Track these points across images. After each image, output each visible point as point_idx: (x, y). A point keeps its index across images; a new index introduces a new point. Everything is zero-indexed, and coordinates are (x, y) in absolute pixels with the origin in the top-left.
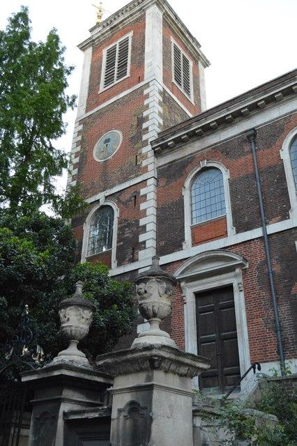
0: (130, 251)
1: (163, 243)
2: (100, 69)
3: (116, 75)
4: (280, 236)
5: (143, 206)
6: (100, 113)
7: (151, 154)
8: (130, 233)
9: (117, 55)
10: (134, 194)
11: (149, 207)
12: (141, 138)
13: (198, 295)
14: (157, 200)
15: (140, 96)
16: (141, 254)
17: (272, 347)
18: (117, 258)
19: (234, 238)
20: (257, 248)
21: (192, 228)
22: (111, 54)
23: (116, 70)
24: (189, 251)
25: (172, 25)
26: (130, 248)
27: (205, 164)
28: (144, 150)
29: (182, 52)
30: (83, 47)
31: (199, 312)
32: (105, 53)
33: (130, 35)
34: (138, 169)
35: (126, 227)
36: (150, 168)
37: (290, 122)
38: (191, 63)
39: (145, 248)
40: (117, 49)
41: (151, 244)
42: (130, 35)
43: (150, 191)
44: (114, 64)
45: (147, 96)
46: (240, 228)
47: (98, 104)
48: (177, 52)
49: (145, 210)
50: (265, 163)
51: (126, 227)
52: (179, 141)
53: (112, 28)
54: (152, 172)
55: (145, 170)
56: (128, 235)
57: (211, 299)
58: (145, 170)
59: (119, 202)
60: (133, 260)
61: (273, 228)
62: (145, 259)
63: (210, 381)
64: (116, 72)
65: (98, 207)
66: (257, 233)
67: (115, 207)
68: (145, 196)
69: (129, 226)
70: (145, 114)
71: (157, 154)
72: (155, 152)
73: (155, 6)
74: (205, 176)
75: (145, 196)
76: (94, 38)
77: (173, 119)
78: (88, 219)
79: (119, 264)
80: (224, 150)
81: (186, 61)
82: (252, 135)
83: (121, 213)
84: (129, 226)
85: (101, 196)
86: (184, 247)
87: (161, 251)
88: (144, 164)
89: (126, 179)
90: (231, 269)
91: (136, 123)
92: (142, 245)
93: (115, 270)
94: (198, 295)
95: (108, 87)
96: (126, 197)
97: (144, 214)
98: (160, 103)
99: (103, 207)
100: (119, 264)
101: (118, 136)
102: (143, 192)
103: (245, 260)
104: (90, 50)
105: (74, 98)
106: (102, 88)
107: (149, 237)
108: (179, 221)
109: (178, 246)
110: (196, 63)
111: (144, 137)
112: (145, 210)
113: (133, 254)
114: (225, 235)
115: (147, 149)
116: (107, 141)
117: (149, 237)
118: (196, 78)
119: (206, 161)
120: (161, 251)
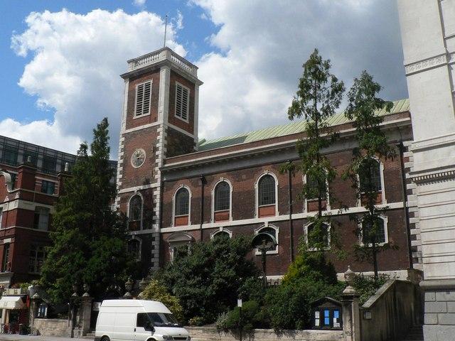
6: (134, 134)
7: (159, 172)
19: (190, 227)
22: (140, 89)
26: (149, 222)
30: (124, 76)
38: (189, 92)
45: (158, 134)
48: (179, 88)
54: (158, 184)
61: (205, 226)
66: (198, 227)
81: (185, 91)
92: (154, 222)
100: (144, 229)
109: (169, 225)
114: (187, 224)
116: (138, 155)
120: (161, 226)
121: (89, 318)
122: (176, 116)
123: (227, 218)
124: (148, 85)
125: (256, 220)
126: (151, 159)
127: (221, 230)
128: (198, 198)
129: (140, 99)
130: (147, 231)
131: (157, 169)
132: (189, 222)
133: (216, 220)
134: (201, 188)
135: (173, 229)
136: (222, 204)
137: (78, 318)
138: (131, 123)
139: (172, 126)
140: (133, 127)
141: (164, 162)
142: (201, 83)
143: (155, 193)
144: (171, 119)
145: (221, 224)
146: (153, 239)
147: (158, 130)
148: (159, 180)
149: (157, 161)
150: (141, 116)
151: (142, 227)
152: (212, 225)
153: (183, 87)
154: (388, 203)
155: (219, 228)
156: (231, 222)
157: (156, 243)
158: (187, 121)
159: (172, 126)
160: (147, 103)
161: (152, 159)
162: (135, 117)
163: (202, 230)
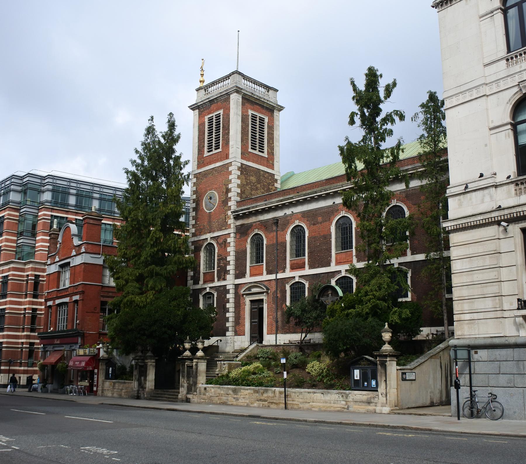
0: (223, 274)
1: (237, 272)
2: (204, 134)
4: (282, 280)
7: (232, 217)
8: (223, 264)
11: (231, 249)
13: (252, 301)
14: (236, 246)
16: (228, 277)
17: (274, 328)
18: (218, 276)
19: (265, 277)
20: (274, 284)
22: (211, 120)
24: (248, 279)
26: (223, 273)
27: (256, 231)
30: (193, 108)
31: (251, 309)
33: (221, 112)
34: (226, 226)
36: (232, 226)
37: (292, 219)
38: (266, 120)
39: (229, 274)
41: (232, 272)
42: (221, 112)
45: (230, 173)
46: (269, 272)
48: (254, 117)
49: (230, 252)
50: (280, 240)
53: (209, 101)
55: (229, 227)
56: (222, 264)
57: (257, 304)
58: (229, 227)
59: (218, 243)
60: (224, 279)
61: (280, 276)
62: (230, 281)
63: (254, 339)
66: (272, 277)
67: (215, 245)
69: (222, 259)
73: (235, 94)
76: (199, 104)
77: (248, 181)
78: (203, 249)
79: (218, 280)
81: (262, 120)
82: (276, 221)
83: (218, 250)
84: (222, 259)
85: (208, 236)
86: (246, 277)
87: (237, 277)
90: (262, 293)
91: (225, 191)
93: (217, 284)
94: (252, 301)
96: (221, 241)
97: (228, 254)
98: (239, 178)
99: (210, 244)
100: (218, 280)
103: (268, 289)
104: (197, 111)
105: (188, 176)
107: (231, 268)
113: (224, 276)
114: (262, 274)
117: (231, 268)
118: (271, 128)
120: (237, 277)
121: (154, 378)
122: (250, 150)
123: (302, 266)
124: (218, 116)
125: (333, 268)
126: (223, 201)
127: (297, 279)
128: (273, 245)
129: (210, 133)
130: (223, 283)
131: (229, 213)
132: (265, 272)
133: (294, 268)
134: (275, 233)
135: (248, 279)
136: (299, 252)
137: (143, 378)
138: (201, 161)
139: (245, 162)
140: (205, 165)
141: (239, 203)
142: (280, 109)
143: (229, 240)
144: (244, 154)
145: (297, 274)
146: (228, 292)
147: (230, 169)
148: (232, 226)
149: (230, 204)
150: (211, 153)
151: (216, 279)
152: (288, 273)
153: (259, 115)
154: (412, 254)
155: (294, 277)
156: (308, 271)
157: (230, 296)
158: (265, 155)
159: (245, 162)
160: (218, 138)
161: (225, 201)
162: (206, 154)
163: (277, 280)
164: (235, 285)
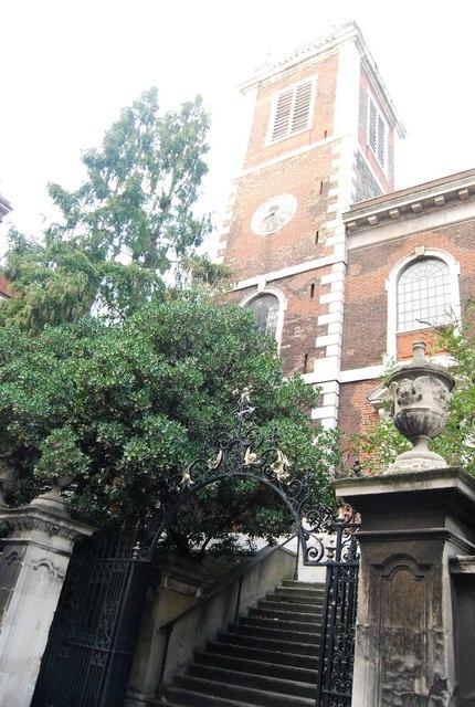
0: (302, 357)
1: (351, 353)
3: (290, 127)
5: (323, 299)
6: (265, 174)
9: (294, 102)
10: (312, 282)
12: (326, 210)
15: (328, 155)
21: (398, 337)
23: (291, 120)
25: (369, 72)
27: (420, 251)
28: (329, 225)
29: (379, 112)
32: (274, 100)
33: (314, 78)
35: (296, 324)
38: (387, 128)
40: (294, 95)
41: (334, 351)
42: (314, 78)
43: (335, 278)
44: (287, 113)
45: (337, 156)
47: (261, 160)
48: (373, 110)
49: (328, 304)
51: (296, 324)
52: (384, 218)
54: (340, 254)
55: (331, 250)
59: (288, 291)
64: (290, 124)
65: (256, 294)
68: (329, 285)
70: (332, 179)
71: (350, 231)
72: (347, 229)
74: (416, 268)
75: (329, 285)
80: (453, 234)
85: (261, 280)
87: (346, 364)
88: (329, 242)
89: (300, 261)
95: (296, 133)
96: (298, 284)
97: (325, 309)
99: (262, 295)
101: (288, 206)
102: (325, 280)
104: (254, 92)
106: (268, 141)
107: (331, 341)
108: (378, 326)
110: (391, 128)
111: (331, 208)
112: (328, 304)
113: (305, 362)
115: (337, 226)
118: (391, 147)
119: (423, 247)
120: (346, 364)
164: (342, 385)
